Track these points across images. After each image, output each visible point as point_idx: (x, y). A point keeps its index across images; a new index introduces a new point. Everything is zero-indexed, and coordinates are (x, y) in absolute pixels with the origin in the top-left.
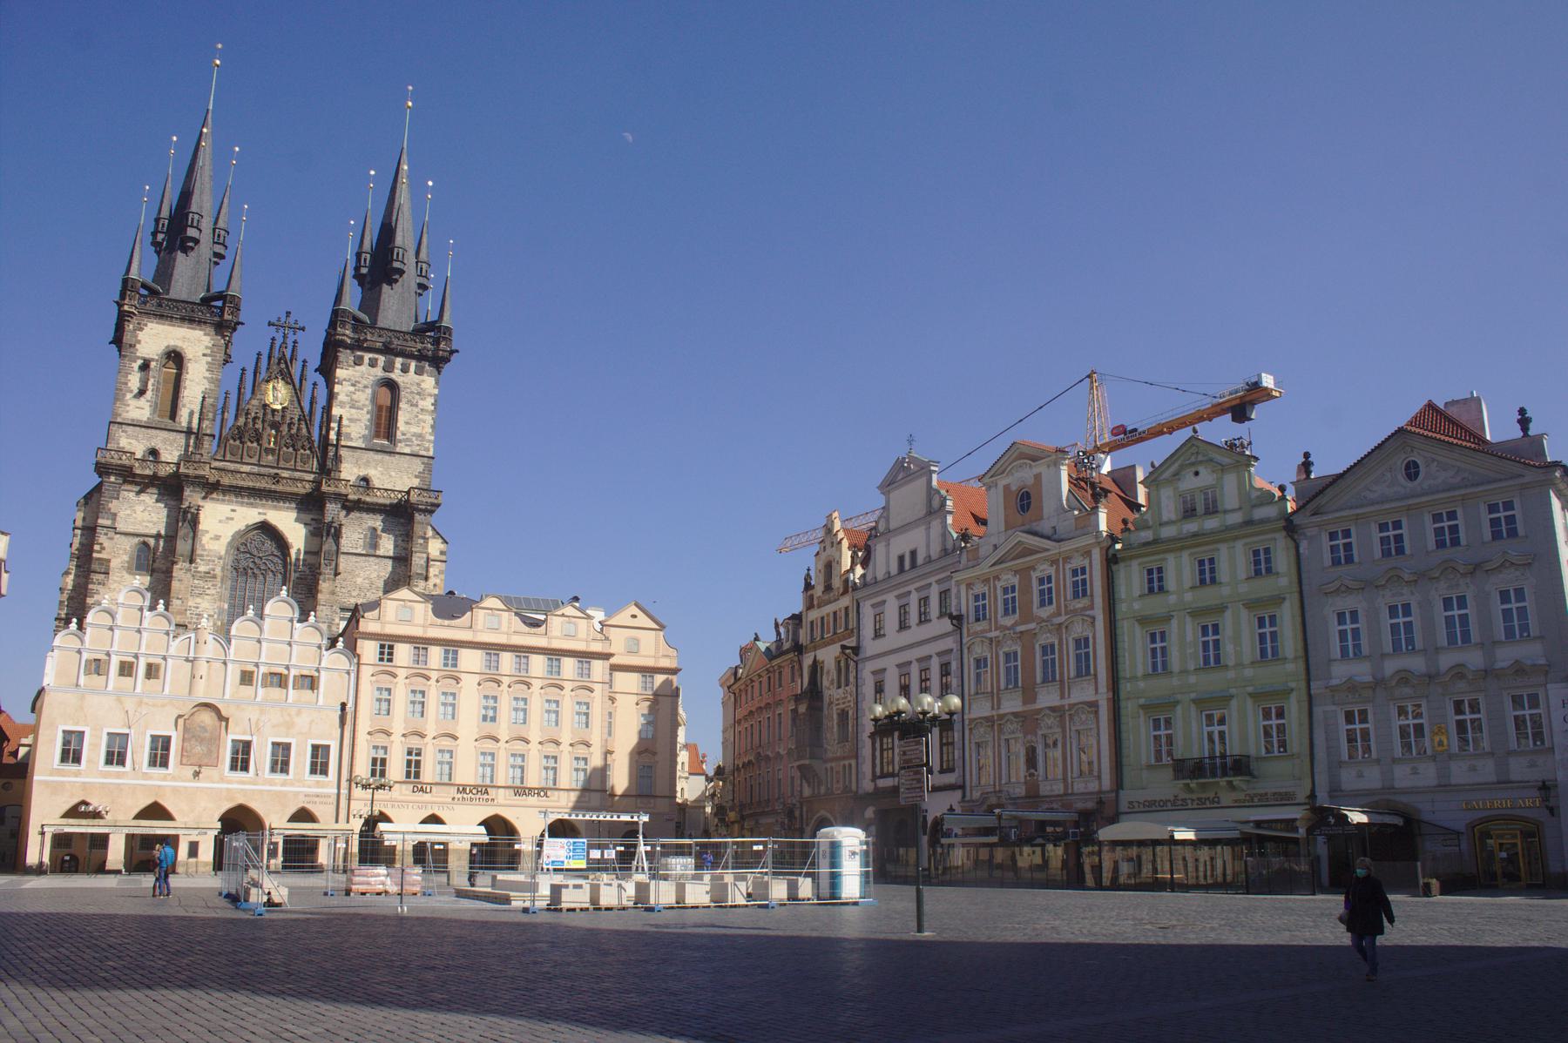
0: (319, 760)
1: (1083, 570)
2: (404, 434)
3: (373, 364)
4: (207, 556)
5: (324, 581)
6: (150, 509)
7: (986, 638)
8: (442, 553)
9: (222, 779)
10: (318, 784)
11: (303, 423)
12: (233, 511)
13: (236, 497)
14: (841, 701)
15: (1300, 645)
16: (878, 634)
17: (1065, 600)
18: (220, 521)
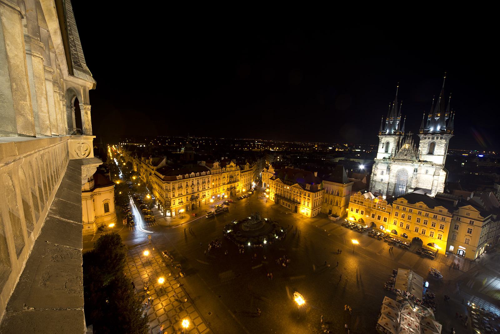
3: (429, 138)
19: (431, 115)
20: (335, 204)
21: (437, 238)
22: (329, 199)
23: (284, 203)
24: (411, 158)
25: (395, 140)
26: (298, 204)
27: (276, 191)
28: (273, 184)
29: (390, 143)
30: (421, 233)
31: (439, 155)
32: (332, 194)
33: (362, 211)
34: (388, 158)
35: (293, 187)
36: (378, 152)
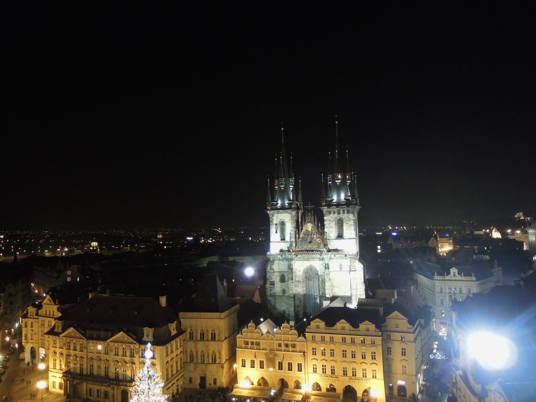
3: (334, 213)
5: (327, 282)
6: (283, 265)
9: (277, 372)
11: (317, 234)
12: (303, 263)
18: (300, 266)
20: (211, 361)
21: (372, 377)
22: (197, 352)
23: (90, 390)
24: (318, 246)
25: (292, 217)
26: (128, 384)
27: (67, 363)
28: (58, 345)
30: (352, 376)
31: (351, 239)
32: (202, 338)
34: (287, 249)
35: (111, 344)
36: (271, 240)
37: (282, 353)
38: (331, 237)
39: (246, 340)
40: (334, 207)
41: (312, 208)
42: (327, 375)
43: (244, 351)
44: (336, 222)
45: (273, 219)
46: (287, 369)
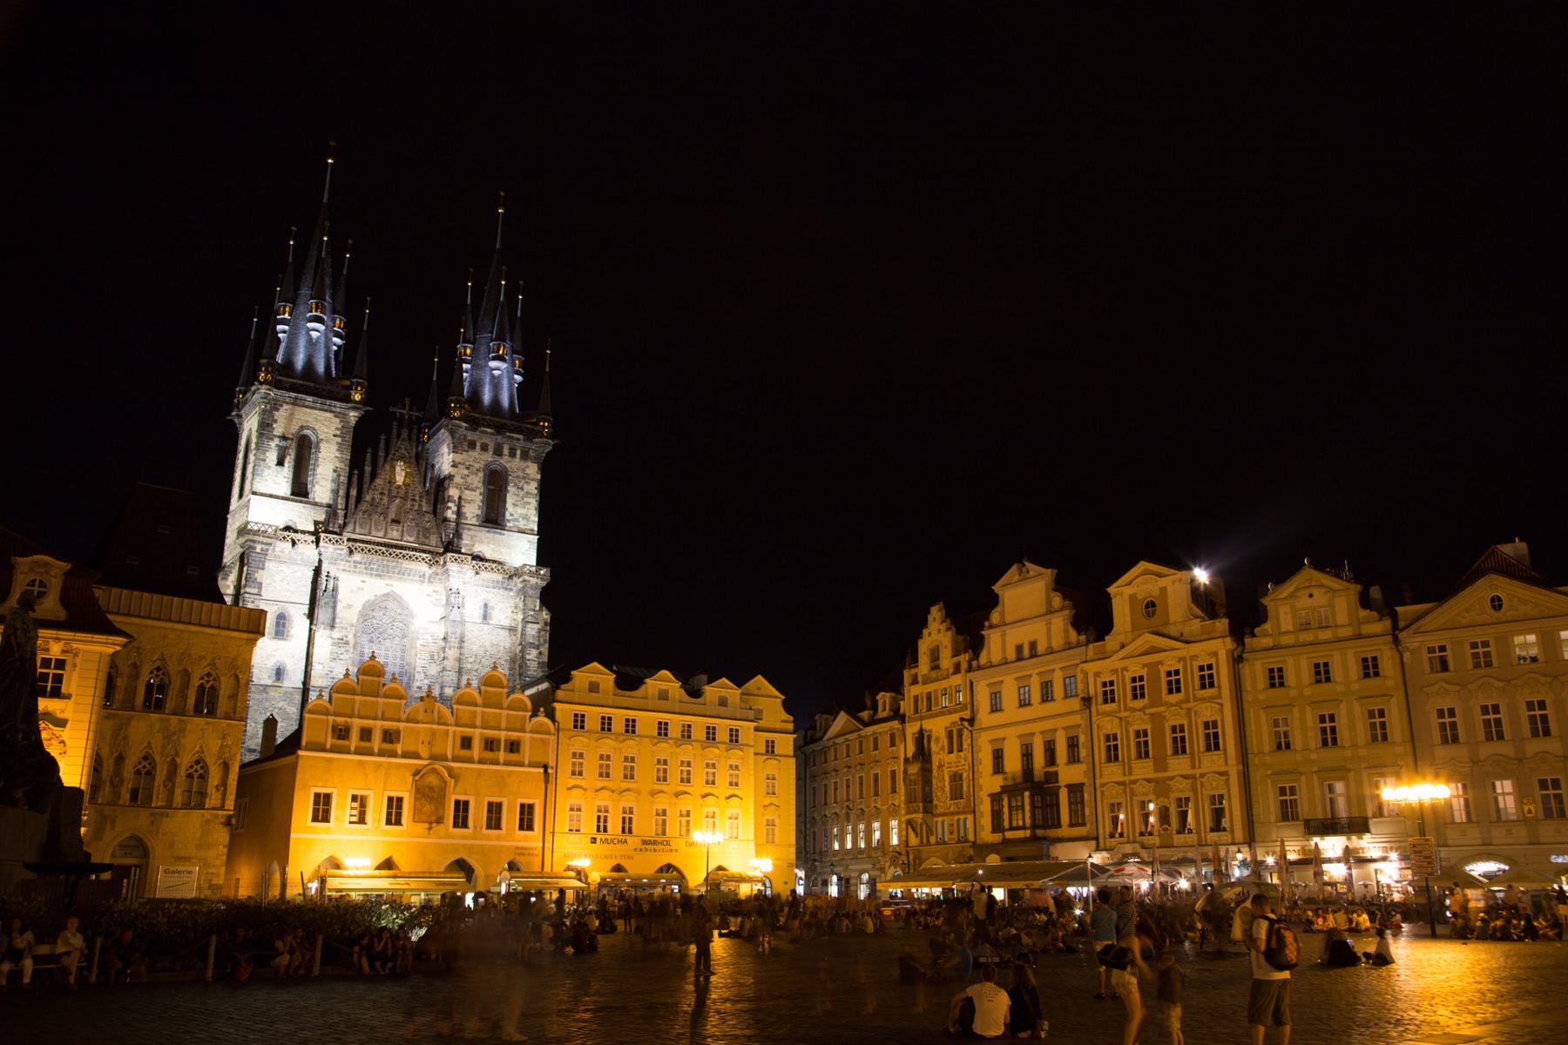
0: (321, 807)
1: (1210, 667)
2: (511, 515)
3: (484, 448)
4: (341, 623)
7: (1117, 717)
8: (546, 624)
9: (448, 836)
10: (526, 839)
11: (424, 500)
12: (363, 582)
13: (366, 568)
14: (953, 765)
15: (1407, 732)
16: (995, 708)
17: (1194, 690)
18: (352, 591)
19: (468, 351)
20: (179, 798)
24: (422, 539)
29: (322, 446)
33: (390, 799)
34: (311, 528)
37: (472, 769)
38: (467, 518)
39: (341, 720)
40: (489, 430)
41: (414, 418)
42: (609, 837)
43: (330, 760)
44: (485, 475)
45: (276, 418)
46: (484, 827)
